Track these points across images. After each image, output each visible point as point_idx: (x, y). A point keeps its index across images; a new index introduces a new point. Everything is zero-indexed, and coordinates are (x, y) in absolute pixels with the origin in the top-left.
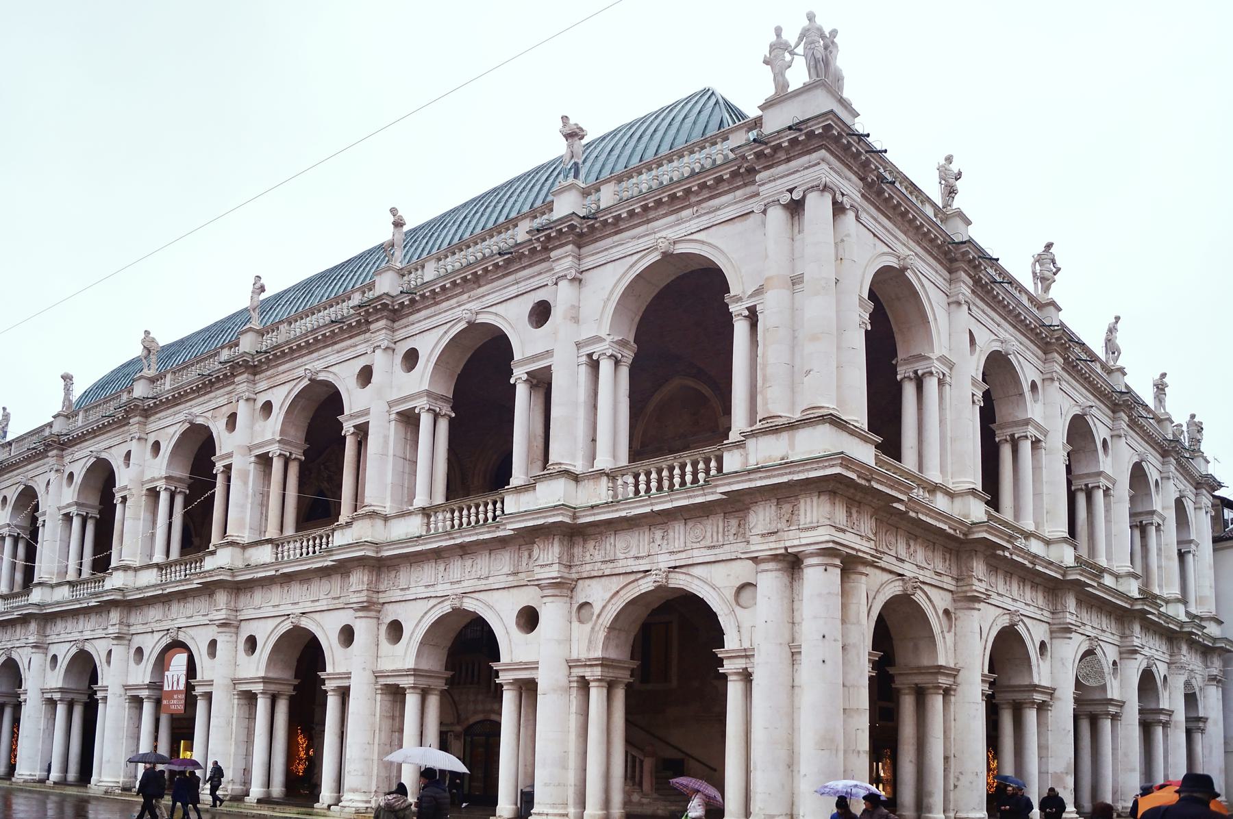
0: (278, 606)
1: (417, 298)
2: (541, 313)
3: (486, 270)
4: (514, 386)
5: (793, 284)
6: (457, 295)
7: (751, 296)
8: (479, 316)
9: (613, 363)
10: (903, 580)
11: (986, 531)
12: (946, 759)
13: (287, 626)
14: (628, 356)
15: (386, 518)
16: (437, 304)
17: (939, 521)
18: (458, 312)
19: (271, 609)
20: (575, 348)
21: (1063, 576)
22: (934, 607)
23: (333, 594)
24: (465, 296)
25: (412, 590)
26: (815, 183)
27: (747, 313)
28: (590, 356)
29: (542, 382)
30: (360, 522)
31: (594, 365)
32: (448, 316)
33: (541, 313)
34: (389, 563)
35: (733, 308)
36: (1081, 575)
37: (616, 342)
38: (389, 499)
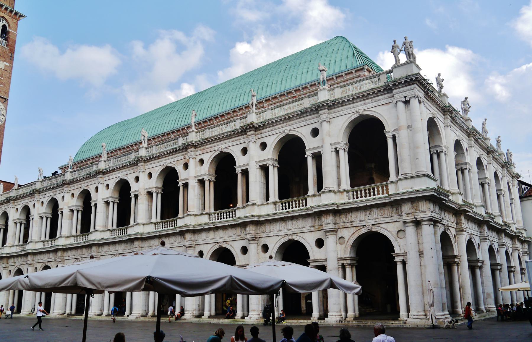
0: (213, 239)
1: (266, 124)
2: (315, 132)
3: (293, 116)
4: (307, 158)
6: (281, 124)
7: (393, 131)
9: (343, 151)
10: (444, 226)
12: (460, 288)
13: (217, 247)
14: (347, 148)
15: (258, 205)
16: (273, 126)
18: (283, 130)
19: (210, 240)
20: (330, 146)
21: (483, 219)
24: (285, 124)
26: (414, 95)
27: (392, 137)
28: (336, 149)
29: (318, 157)
30: (249, 207)
31: (337, 152)
32: (278, 131)
33: (315, 132)
35: (387, 135)
36: (489, 218)
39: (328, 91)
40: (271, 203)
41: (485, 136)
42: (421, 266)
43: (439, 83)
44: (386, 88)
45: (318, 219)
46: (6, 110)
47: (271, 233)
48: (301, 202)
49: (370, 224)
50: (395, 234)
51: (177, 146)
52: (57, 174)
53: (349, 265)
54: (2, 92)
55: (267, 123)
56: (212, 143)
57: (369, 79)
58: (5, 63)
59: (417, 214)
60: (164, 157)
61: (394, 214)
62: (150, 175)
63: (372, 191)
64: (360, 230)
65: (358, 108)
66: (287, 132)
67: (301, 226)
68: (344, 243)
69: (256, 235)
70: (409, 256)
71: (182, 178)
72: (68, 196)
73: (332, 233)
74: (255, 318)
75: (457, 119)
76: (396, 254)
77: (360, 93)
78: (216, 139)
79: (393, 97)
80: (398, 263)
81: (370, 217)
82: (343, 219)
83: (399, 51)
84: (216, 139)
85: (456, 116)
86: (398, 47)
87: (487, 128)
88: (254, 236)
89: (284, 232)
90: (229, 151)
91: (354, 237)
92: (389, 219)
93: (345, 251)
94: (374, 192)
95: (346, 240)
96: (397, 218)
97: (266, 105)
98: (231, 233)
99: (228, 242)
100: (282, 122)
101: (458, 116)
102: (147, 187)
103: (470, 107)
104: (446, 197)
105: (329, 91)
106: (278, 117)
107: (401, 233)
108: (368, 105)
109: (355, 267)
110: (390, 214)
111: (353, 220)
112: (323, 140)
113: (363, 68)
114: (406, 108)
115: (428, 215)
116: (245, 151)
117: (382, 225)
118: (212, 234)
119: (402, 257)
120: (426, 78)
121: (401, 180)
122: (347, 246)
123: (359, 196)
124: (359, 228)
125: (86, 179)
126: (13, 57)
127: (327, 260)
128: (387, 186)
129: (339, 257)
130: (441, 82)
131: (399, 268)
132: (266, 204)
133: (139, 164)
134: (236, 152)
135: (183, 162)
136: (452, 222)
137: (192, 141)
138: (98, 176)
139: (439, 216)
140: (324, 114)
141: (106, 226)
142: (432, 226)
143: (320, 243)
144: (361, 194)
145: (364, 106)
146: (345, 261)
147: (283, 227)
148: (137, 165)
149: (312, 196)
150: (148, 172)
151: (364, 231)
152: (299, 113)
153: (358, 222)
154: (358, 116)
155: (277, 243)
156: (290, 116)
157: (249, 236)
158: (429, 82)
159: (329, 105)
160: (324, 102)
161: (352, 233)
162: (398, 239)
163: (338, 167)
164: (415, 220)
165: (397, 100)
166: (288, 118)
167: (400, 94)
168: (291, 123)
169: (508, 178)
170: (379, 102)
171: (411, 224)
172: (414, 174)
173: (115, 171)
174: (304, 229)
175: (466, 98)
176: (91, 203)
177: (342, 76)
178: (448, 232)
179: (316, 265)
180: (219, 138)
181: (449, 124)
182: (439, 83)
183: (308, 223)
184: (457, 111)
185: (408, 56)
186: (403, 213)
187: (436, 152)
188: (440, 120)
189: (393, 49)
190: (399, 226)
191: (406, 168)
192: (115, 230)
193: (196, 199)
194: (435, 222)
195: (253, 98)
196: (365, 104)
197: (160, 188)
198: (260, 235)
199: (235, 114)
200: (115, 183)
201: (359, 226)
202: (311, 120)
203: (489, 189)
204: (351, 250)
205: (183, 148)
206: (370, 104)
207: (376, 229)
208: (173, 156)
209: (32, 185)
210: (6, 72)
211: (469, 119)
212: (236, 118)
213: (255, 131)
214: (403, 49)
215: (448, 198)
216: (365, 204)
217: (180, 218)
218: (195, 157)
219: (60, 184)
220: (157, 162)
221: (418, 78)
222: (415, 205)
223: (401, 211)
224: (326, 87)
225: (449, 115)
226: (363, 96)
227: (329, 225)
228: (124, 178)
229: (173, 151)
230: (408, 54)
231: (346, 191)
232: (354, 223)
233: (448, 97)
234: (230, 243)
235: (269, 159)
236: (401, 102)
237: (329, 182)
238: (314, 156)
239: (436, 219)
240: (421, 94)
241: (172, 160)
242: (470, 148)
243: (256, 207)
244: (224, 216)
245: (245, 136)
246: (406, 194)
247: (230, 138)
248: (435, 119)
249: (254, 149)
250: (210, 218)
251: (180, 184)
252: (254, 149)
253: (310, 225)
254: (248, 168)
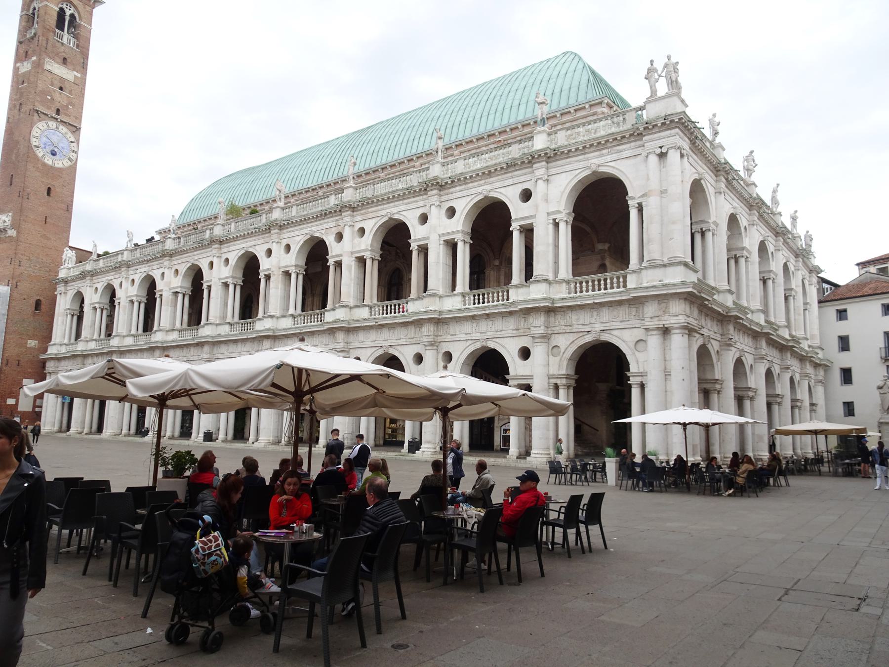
0: (374, 341)
1: (456, 180)
2: (526, 195)
4: (512, 232)
5: (661, 194)
7: (639, 197)
8: (491, 193)
11: (737, 312)
14: (570, 220)
15: (441, 297)
16: (466, 184)
17: (719, 307)
18: (480, 189)
19: (370, 343)
21: (761, 330)
22: (714, 350)
23: (409, 336)
24: (483, 182)
27: (637, 205)
28: (554, 220)
29: (528, 232)
31: (556, 225)
32: (473, 191)
33: (526, 195)
34: (444, 321)
35: (630, 202)
36: (770, 330)
37: (567, 214)
38: (441, 287)
39: (548, 134)
40: (458, 295)
41: (774, 210)
42: (666, 391)
43: (713, 127)
44: (634, 132)
45: (523, 319)
46: (78, 144)
47: (457, 336)
48: (500, 294)
49: (598, 329)
50: (632, 345)
51: (327, 207)
52: (153, 240)
53: (565, 385)
54: (72, 117)
55: (458, 179)
56: (377, 206)
57: (609, 118)
58: (75, 73)
59: (666, 318)
60: (308, 223)
61: (632, 317)
62: (288, 248)
63: (602, 282)
64: (583, 338)
65: (590, 161)
66: (485, 193)
67: (500, 328)
68: (559, 354)
69: (436, 338)
70: (649, 377)
71: (334, 254)
72: (169, 273)
73: (542, 340)
74: (430, 453)
75: (735, 182)
76: (632, 373)
77: (595, 139)
78: (383, 199)
79: (644, 146)
80: (632, 386)
81: (598, 320)
82: (559, 322)
83: (657, 77)
84: (383, 199)
85: (734, 179)
86: (656, 71)
87: (780, 196)
88: (432, 340)
89: (475, 336)
90: (402, 218)
91: (574, 348)
92: (626, 323)
93: (559, 366)
94: (606, 284)
95: (562, 351)
96: (637, 323)
97: (456, 152)
98: (401, 333)
99: (396, 347)
100: (479, 178)
101: (737, 178)
102: (282, 265)
103: (756, 165)
104: (709, 296)
105: (549, 134)
106: (473, 171)
107: (641, 344)
108: (606, 157)
109: (572, 388)
110: (627, 317)
111: (574, 323)
112: (537, 206)
113: (602, 101)
114: (662, 163)
115: (681, 320)
116: (424, 219)
117: (615, 332)
118: (373, 335)
119: (640, 378)
120: (693, 120)
121: (645, 268)
122: (563, 359)
123: (584, 289)
124: (581, 334)
125: (195, 249)
126: (87, 65)
127: (534, 377)
128: (625, 277)
129: (551, 373)
130: (716, 127)
131: (635, 393)
132: (451, 296)
133: (272, 232)
134: (411, 219)
135: (335, 231)
136: (715, 333)
137: (349, 202)
138: (213, 247)
139: (697, 322)
140: (540, 169)
141: (224, 317)
142: (687, 336)
143: (525, 353)
144: (587, 286)
145: (600, 159)
146: (559, 380)
147: (474, 329)
148: (270, 232)
149: (517, 286)
150: (284, 242)
151: (588, 339)
152: (505, 166)
153: (580, 326)
154: (590, 173)
155: (464, 350)
156: (491, 171)
157: (425, 339)
158: (699, 125)
159: (549, 155)
160: (541, 150)
161: (571, 341)
162: (637, 353)
163: (556, 246)
164: (662, 326)
165: (648, 151)
166: (488, 173)
167: (653, 142)
168: (492, 179)
169: (802, 273)
170: (622, 153)
171: (654, 333)
172: (666, 261)
173: (238, 240)
174: (503, 332)
175: (752, 152)
176: (202, 284)
177: (570, 112)
178: (709, 346)
179: (518, 384)
180: (388, 198)
181: (722, 190)
182: (713, 127)
183: (510, 325)
184: (736, 171)
185: (670, 85)
186: (647, 315)
187: (700, 230)
188: (710, 183)
189: (648, 73)
190: (639, 334)
191: (653, 252)
192: (236, 323)
193: (352, 285)
194: (690, 331)
195: (439, 141)
196: (601, 156)
197: (301, 267)
198: (440, 338)
199: (412, 164)
200: (237, 257)
201: (581, 332)
202: (521, 177)
203: (774, 288)
204: (568, 365)
205: (335, 211)
206: (608, 156)
207: (606, 337)
208: (321, 222)
209: (117, 255)
210: (76, 86)
211: (754, 184)
212: (412, 169)
213: (440, 191)
214: (664, 74)
215: (712, 298)
216: (591, 302)
217: (329, 310)
218: (353, 224)
219: (159, 256)
220: (297, 230)
221: (682, 118)
222: (664, 305)
223: (643, 313)
224: (546, 128)
225: (723, 176)
226: (599, 143)
227: (540, 329)
228: (251, 250)
229: (321, 215)
230: (670, 82)
231: (566, 282)
232: (575, 327)
233: (724, 149)
234: (399, 348)
235: (457, 232)
236: (654, 155)
237: (540, 267)
238: (522, 230)
239: (692, 327)
240: (685, 145)
241: (321, 227)
242: (751, 226)
243: (437, 299)
244: (391, 309)
245: (425, 197)
246: (652, 289)
247: (404, 199)
248: (702, 181)
249: (437, 216)
250: (371, 312)
251: (331, 262)
252: (437, 216)
253: (511, 327)
254: (427, 244)
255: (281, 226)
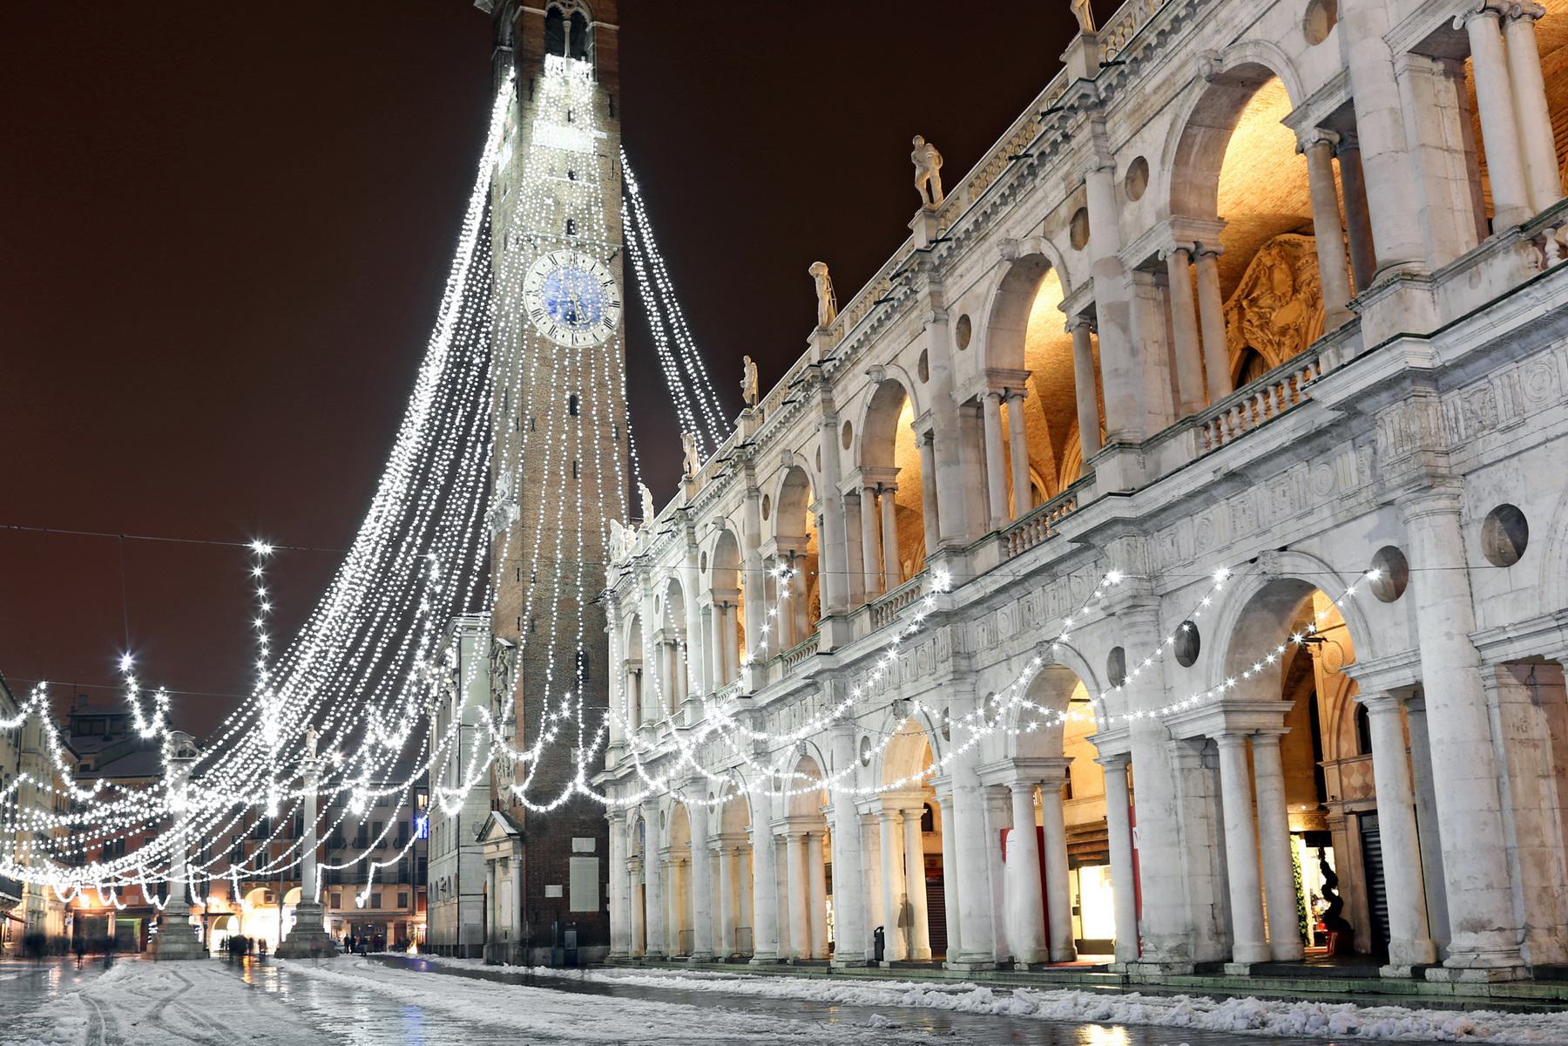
25: (1535, 423)
135: (1065, 212)
218: (1108, 163)
255: (936, 269)
